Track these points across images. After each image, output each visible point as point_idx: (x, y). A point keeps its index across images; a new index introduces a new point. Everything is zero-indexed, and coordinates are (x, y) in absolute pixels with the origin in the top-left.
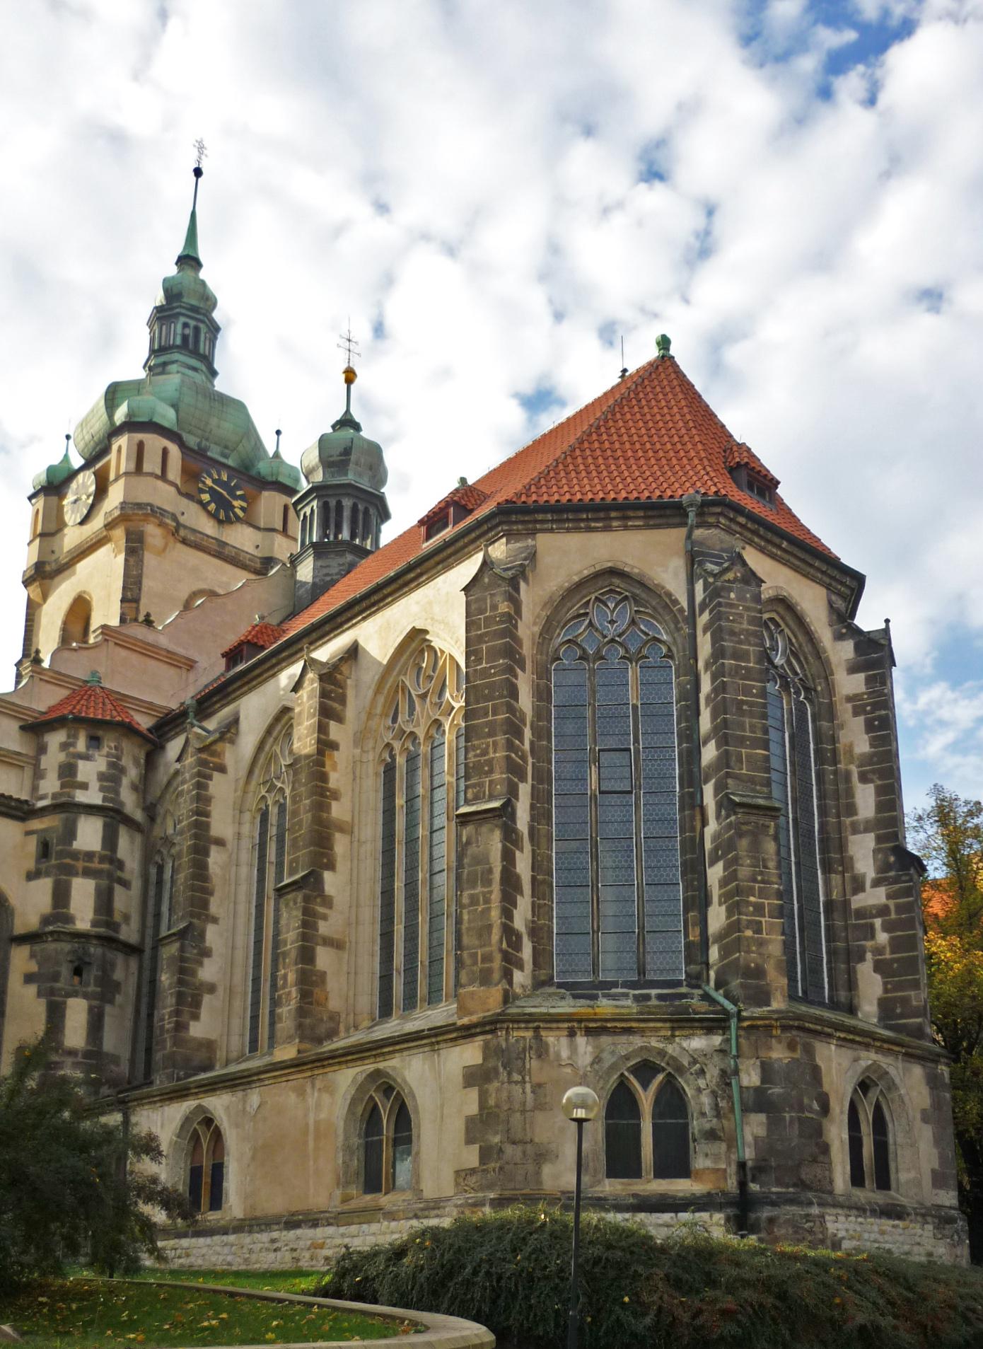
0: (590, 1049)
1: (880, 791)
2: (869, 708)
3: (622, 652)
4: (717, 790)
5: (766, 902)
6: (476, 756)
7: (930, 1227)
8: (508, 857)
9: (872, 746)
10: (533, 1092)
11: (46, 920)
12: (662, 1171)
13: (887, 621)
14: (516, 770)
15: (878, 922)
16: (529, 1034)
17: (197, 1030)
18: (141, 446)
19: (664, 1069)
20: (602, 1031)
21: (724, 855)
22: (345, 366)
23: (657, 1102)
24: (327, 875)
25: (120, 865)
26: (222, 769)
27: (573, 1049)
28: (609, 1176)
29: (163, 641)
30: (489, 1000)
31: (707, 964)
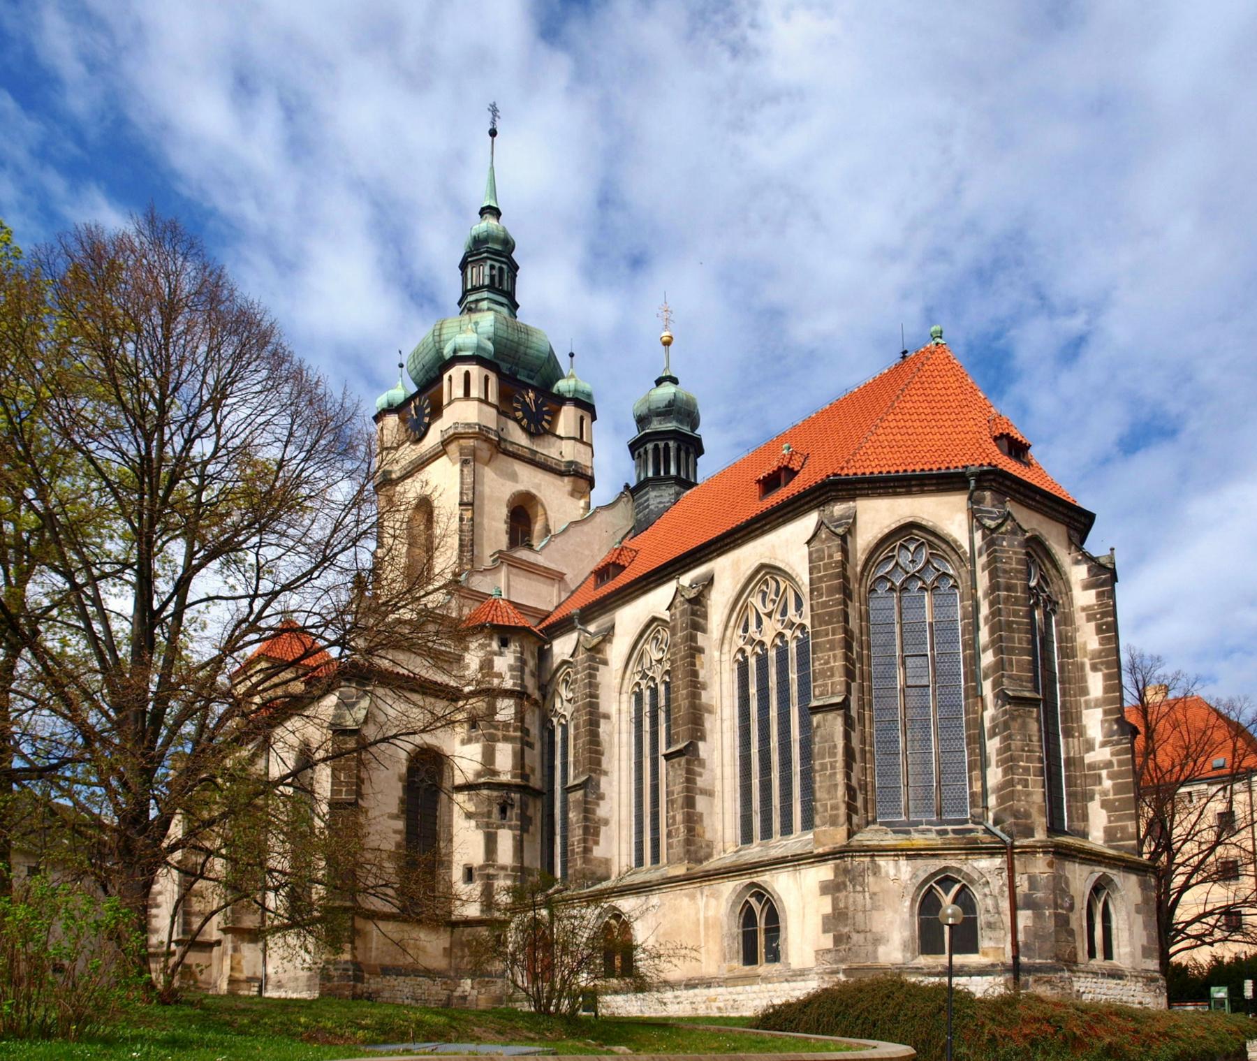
1: (1107, 677)
3: (920, 584)
6: (821, 664)
13: (1112, 549)
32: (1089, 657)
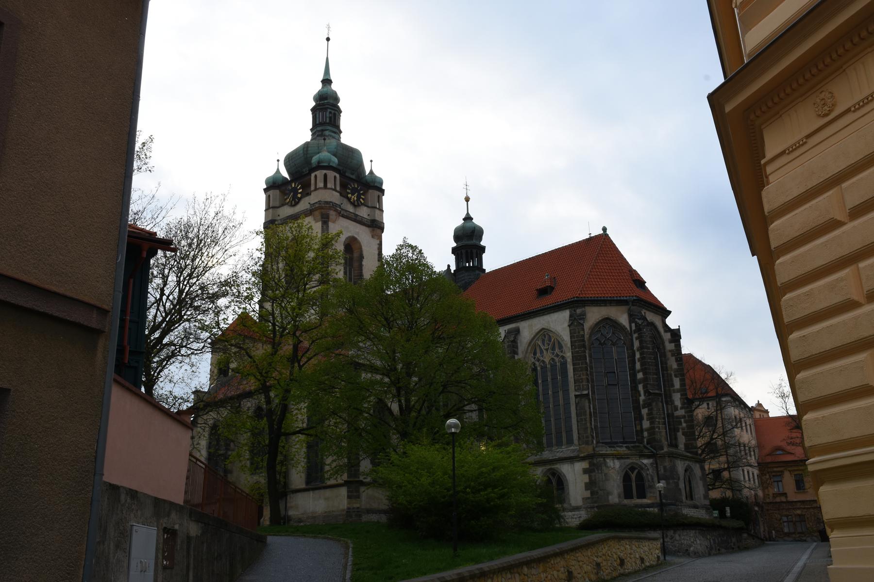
0: (618, 463)
1: (681, 380)
2: (676, 354)
7: (704, 511)
9: (678, 366)
10: (605, 476)
12: (638, 498)
13: (679, 326)
15: (683, 420)
16: (602, 459)
20: (622, 458)
23: (636, 477)
27: (614, 463)
28: (625, 499)
30: (589, 450)
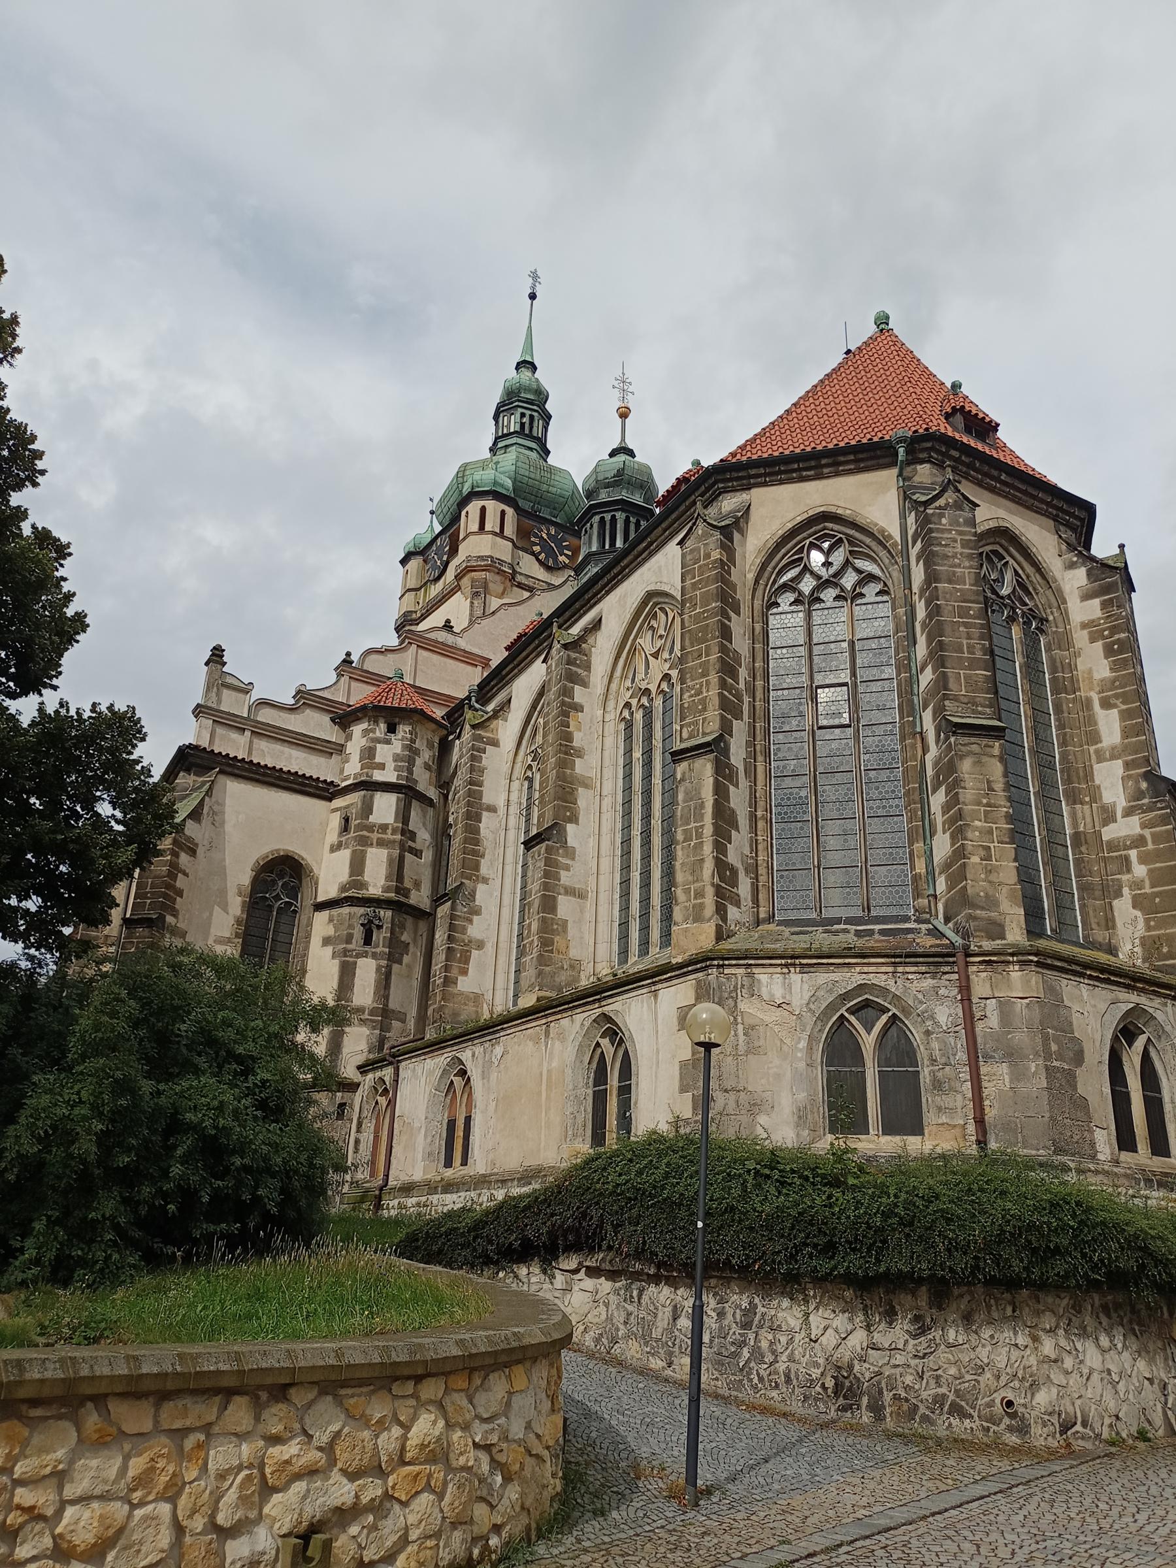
1: (1125, 715)
4: (939, 711)
5: (994, 826)
6: (691, 696)
8: (720, 792)
11: (343, 888)
12: (889, 1129)
14: (730, 708)
17: (464, 984)
18: (483, 510)
19: (885, 1010)
21: (946, 779)
22: (619, 404)
24: (570, 828)
25: (412, 836)
26: (495, 743)
29: (462, 643)
31: (935, 896)
32: (1097, 689)
